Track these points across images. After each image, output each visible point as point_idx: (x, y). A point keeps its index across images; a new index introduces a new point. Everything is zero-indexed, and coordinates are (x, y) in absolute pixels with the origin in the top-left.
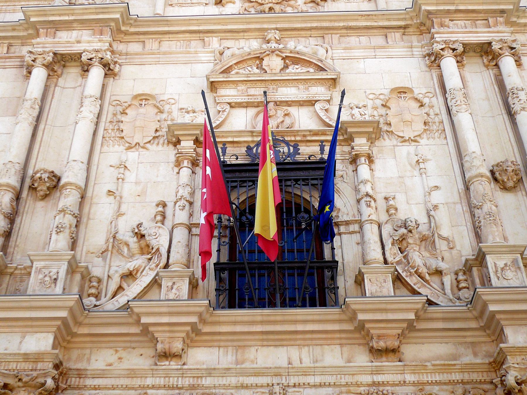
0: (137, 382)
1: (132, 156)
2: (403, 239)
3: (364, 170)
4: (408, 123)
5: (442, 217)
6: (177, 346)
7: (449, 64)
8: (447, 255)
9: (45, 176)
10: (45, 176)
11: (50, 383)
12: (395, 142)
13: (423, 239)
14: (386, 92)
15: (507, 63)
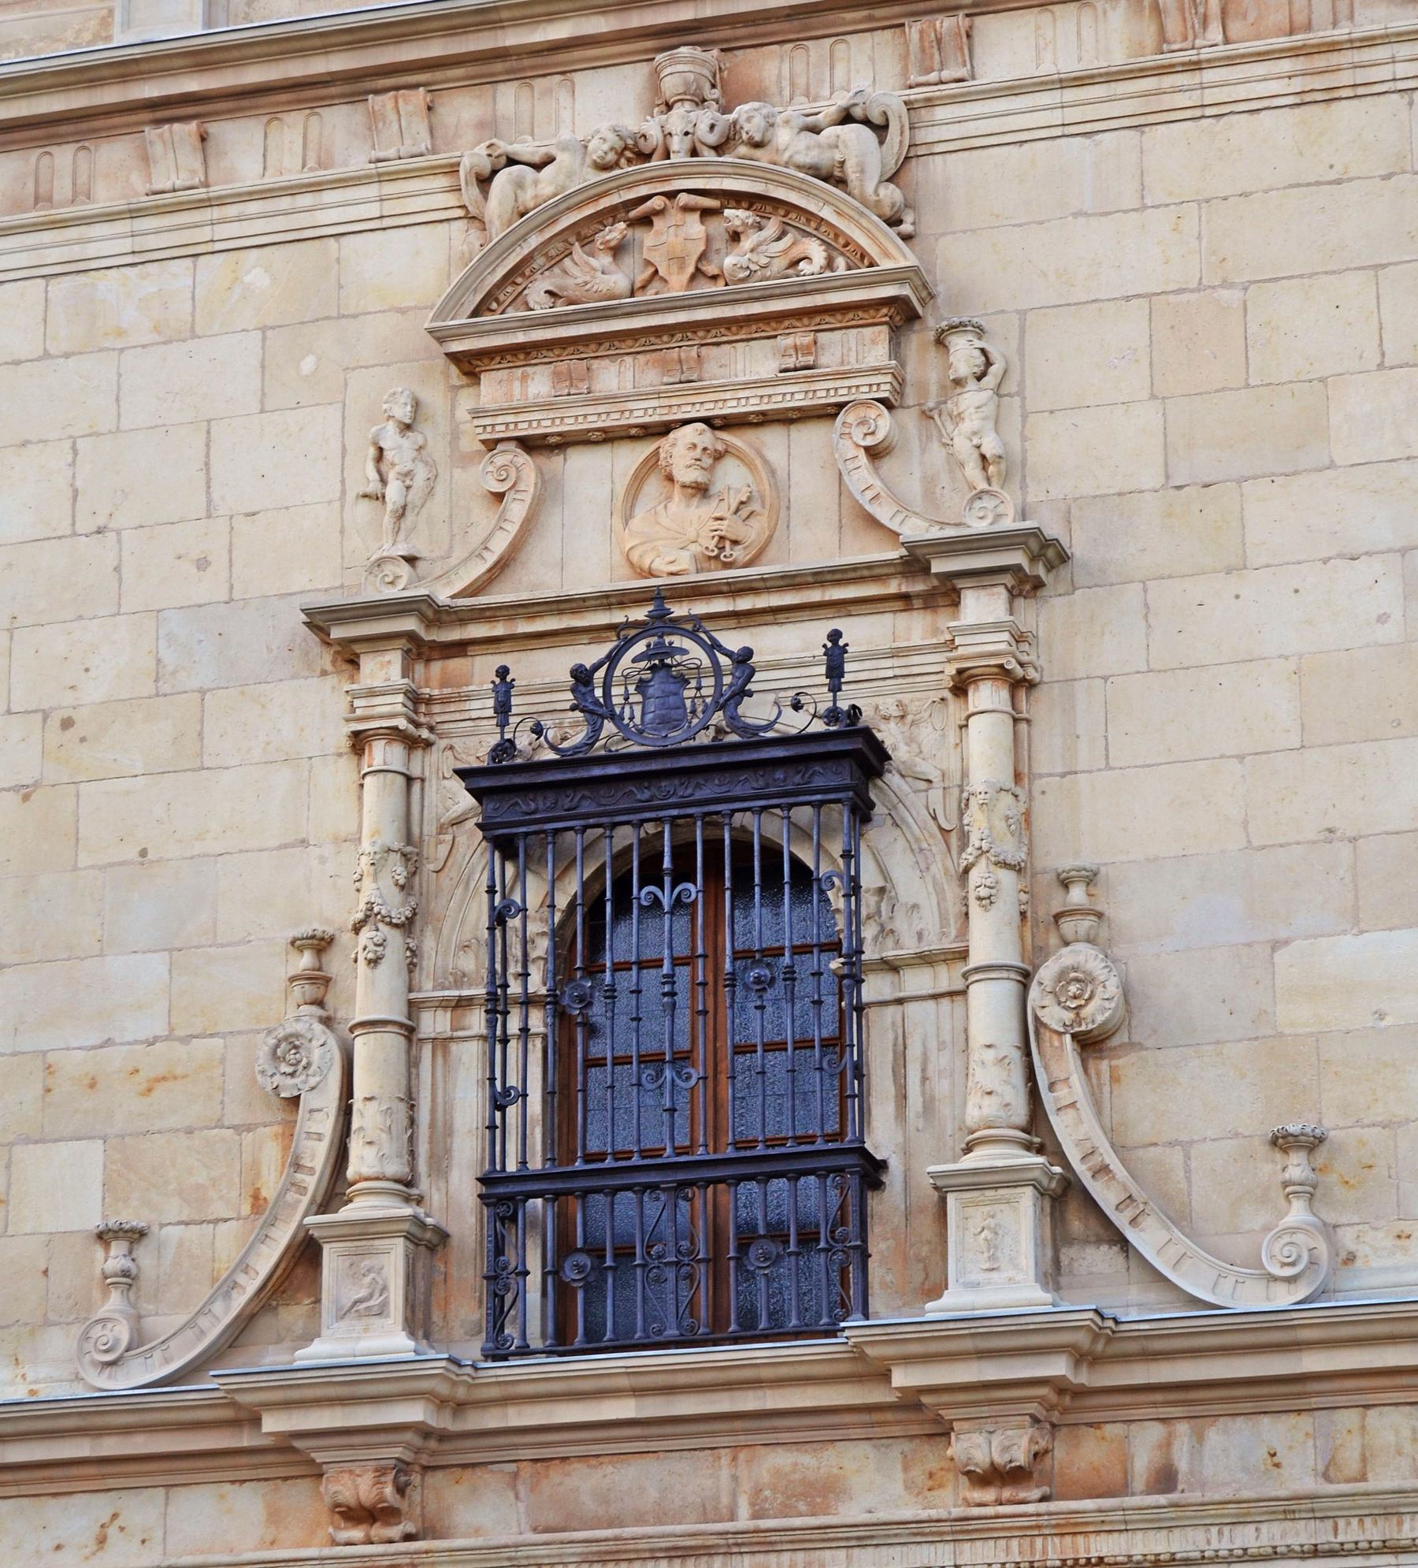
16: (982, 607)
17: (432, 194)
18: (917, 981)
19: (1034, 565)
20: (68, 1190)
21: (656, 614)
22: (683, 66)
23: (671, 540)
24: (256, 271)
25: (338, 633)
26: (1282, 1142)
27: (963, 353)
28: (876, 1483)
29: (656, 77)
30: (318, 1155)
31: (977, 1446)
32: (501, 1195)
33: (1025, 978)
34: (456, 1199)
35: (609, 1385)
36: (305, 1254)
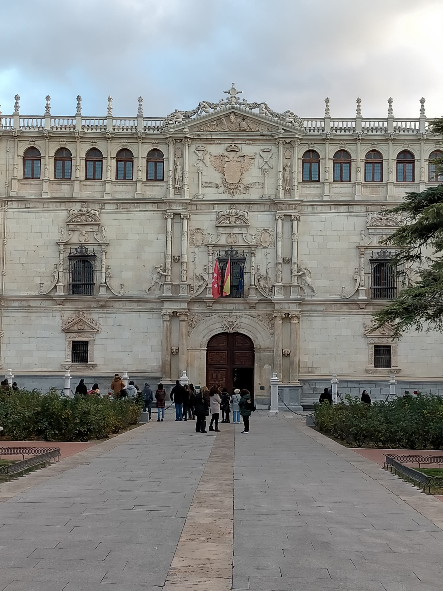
0: (203, 311)
1: (197, 249)
2: (259, 279)
3: (253, 258)
4: (265, 242)
5: (270, 272)
6: (211, 305)
7: (280, 222)
8: (269, 282)
9: (177, 258)
10: (177, 258)
11: (188, 314)
12: (262, 247)
13: (264, 278)
14: (262, 229)
15: (295, 222)
16: (103, 247)
17: (65, 211)
18: (98, 272)
19: (107, 244)
20: (38, 280)
21: (82, 245)
22: (85, 205)
23: (82, 239)
24: (52, 214)
25: (58, 244)
26: (121, 285)
27: (103, 230)
28: (94, 305)
29: (82, 205)
30: (57, 280)
31: (101, 303)
32: (70, 284)
33: (105, 273)
34: (66, 283)
35: (76, 297)
36: (56, 286)
